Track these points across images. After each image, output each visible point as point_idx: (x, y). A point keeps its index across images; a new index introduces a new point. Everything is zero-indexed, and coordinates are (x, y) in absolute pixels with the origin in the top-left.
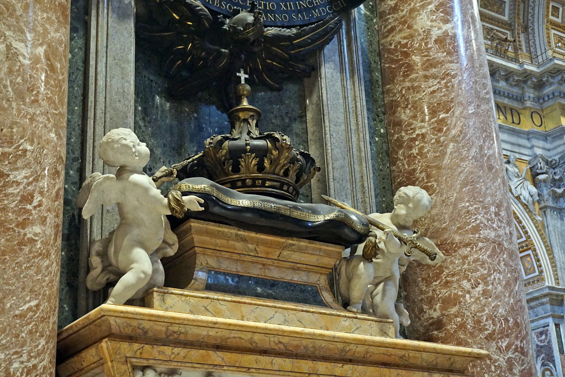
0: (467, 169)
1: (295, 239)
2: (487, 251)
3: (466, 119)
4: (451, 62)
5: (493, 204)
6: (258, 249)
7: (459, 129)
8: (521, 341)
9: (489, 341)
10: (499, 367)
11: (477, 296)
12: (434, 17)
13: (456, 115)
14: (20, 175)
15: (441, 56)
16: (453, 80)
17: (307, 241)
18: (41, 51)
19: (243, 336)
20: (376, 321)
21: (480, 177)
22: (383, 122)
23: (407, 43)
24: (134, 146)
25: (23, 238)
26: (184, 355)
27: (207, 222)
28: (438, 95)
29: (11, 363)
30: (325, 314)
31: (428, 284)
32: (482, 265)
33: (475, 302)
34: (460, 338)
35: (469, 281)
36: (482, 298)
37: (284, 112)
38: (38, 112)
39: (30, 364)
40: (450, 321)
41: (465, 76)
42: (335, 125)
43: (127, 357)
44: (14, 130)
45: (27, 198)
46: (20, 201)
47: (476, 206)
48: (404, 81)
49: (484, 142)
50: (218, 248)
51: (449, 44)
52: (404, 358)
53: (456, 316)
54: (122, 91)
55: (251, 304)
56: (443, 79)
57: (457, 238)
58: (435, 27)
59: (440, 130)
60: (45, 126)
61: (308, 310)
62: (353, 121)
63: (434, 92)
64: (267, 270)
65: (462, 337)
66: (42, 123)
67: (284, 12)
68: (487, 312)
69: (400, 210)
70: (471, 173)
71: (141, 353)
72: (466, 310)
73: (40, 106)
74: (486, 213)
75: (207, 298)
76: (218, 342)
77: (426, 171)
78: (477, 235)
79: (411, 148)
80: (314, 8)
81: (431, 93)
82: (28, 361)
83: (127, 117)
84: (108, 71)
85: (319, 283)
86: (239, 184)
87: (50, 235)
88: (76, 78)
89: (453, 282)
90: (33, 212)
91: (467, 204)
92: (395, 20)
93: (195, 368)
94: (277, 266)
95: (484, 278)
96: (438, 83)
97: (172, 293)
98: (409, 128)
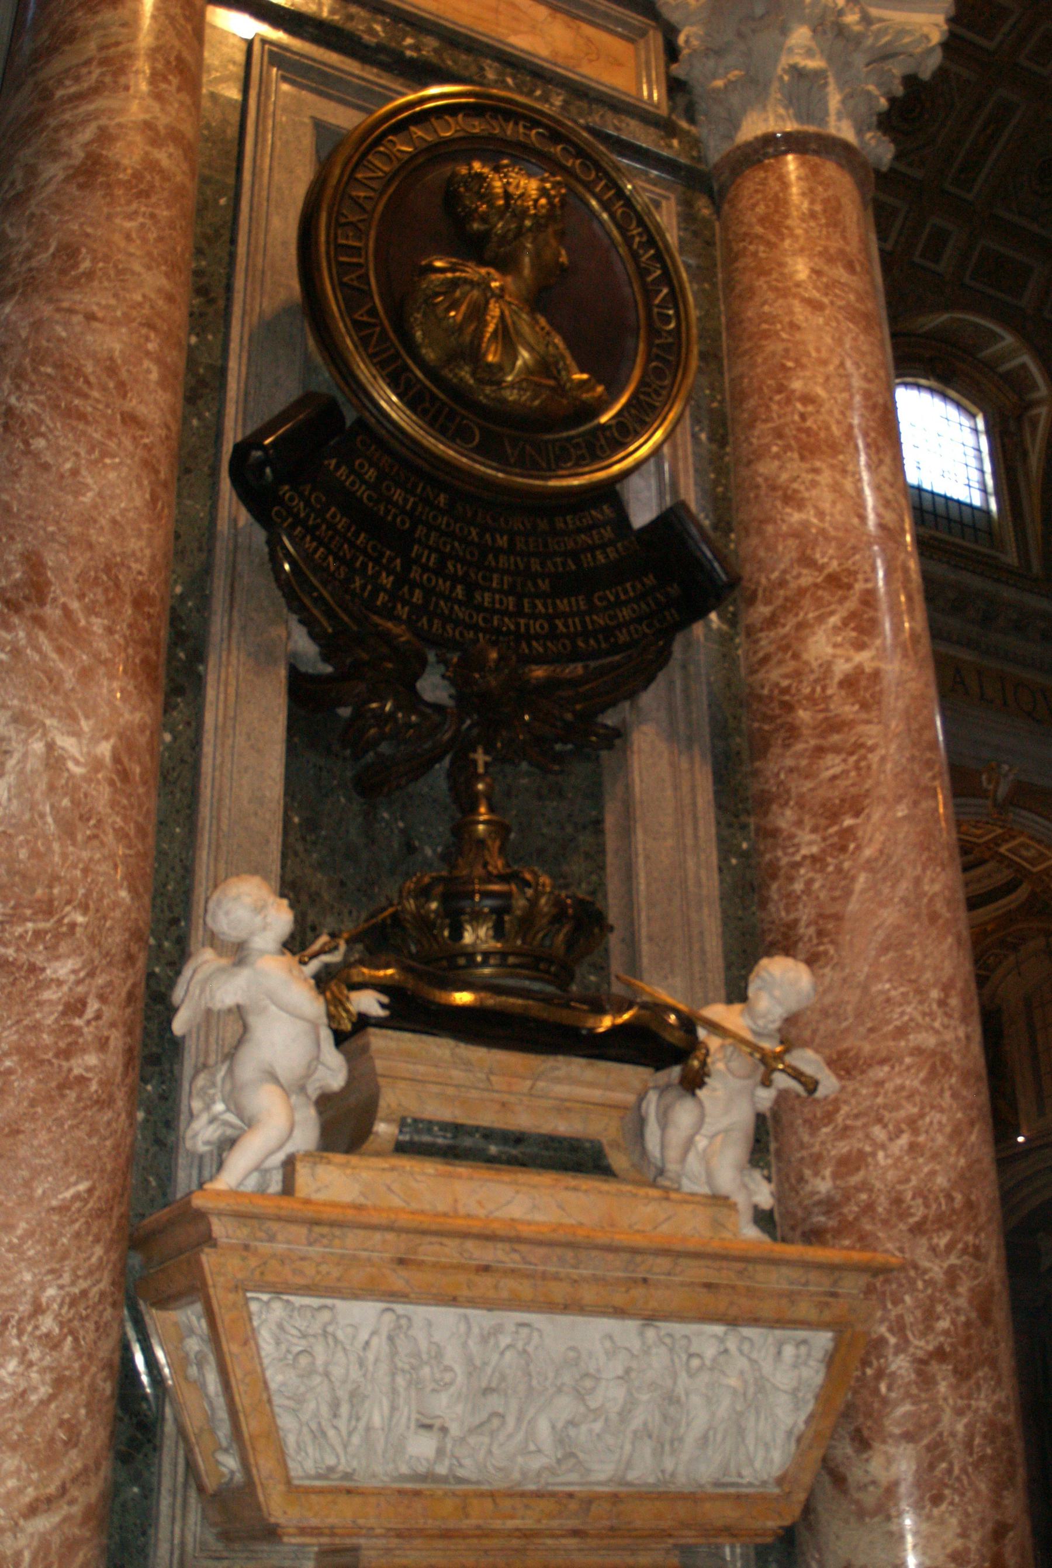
2: (919, 1071)
4: (868, 722)
5: (934, 985)
8: (976, 1235)
11: (897, 1152)
12: (839, 639)
15: (849, 710)
16: (870, 756)
18: (105, 749)
21: (913, 935)
23: (789, 687)
25: (67, 1077)
28: (842, 783)
29: (42, 1287)
31: (814, 1130)
33: (895, 1166)
35: (885, 1126)
38: (98, 856)
39: (76, 1290)
41: (893, 747)
44: (56, 891)
46: (64, 1013)
48: (783, 756)
51: (866, 689)
56: (852, 754)
57: (867, 1048)
58: (841, 656)
59: (843, 849)
62: (689, 831)
63: (834, 778)
65: (868, 1227)
66: (105, 874)
68: (914, 1181)
71: (262, 1273)
74: (921, 1002)
79: (791, 879)
80: (619, 627)
82: (73, 1283)
87: (116, 1068)
90: (86, 1030)
91: (887, 986)
92: (770, 643)
95: (912, 1123)
98: (788, 843)
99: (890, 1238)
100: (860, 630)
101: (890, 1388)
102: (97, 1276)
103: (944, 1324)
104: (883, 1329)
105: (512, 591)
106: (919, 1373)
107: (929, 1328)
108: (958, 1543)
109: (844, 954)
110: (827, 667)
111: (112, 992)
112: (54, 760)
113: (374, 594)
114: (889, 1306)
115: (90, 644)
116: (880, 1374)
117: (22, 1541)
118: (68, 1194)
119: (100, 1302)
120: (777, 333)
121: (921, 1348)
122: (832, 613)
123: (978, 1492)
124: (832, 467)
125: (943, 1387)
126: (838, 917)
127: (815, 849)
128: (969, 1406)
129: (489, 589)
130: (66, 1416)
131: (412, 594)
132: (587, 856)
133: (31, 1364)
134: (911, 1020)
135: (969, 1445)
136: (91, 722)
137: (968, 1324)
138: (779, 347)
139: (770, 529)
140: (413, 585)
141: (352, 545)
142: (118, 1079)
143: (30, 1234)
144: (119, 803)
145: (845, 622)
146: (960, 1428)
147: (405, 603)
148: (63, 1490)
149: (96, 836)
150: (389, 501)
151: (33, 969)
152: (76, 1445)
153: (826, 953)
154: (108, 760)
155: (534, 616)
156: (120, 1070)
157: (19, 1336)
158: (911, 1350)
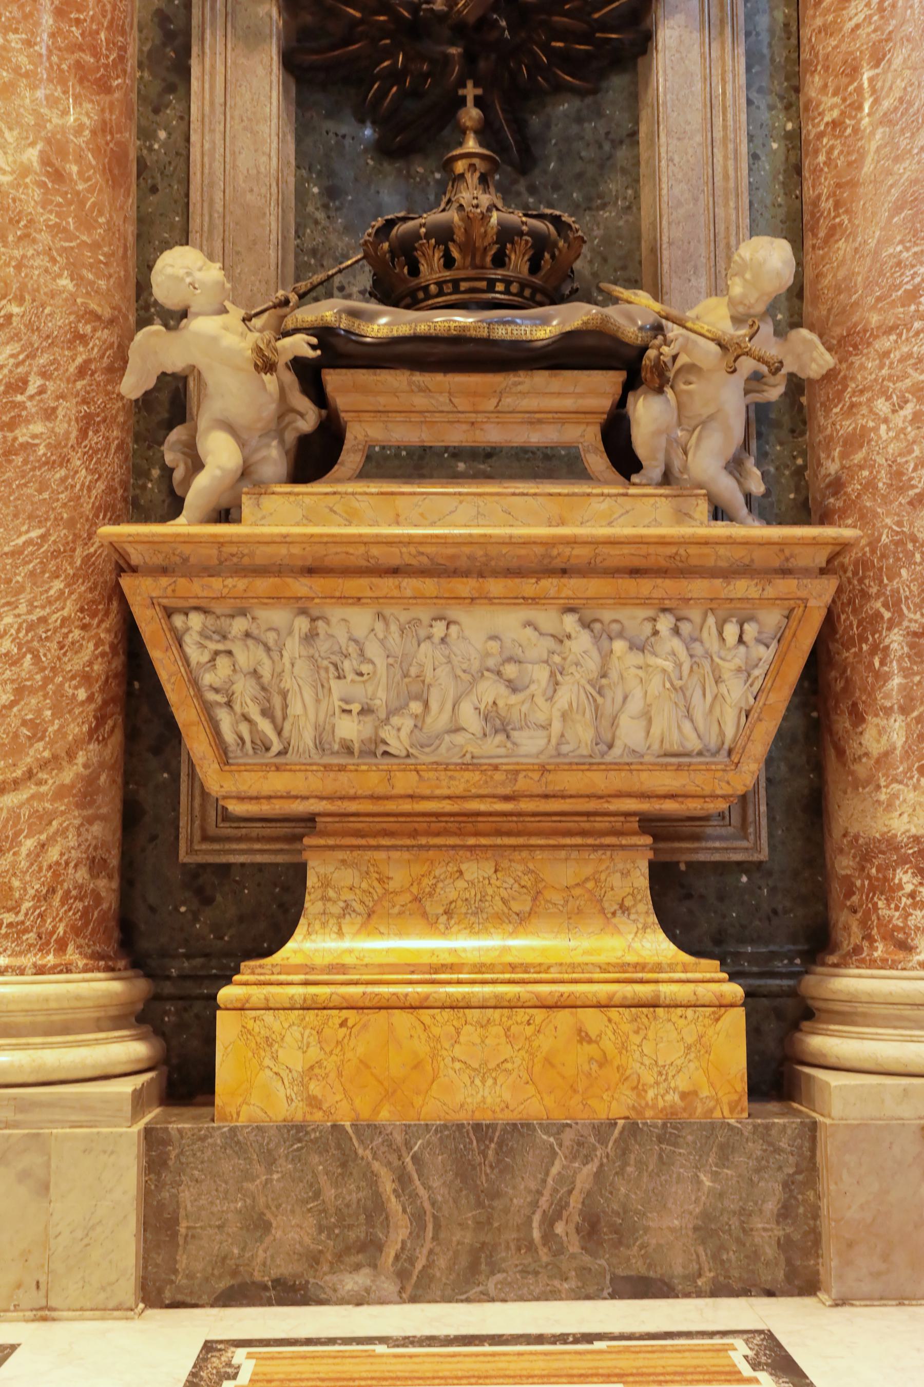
0: (906, 176)
1: (521, 373)
3: (915, 69)
6: (455, 400)
7: (898, 95)
9: (914, 507)
11: (901, 425)
13: (893, 67)
17: (546, 373)
18: (32, 155)
19: (351, 551)
20: (666, 496)
22: (794, 108)
24: (188, 274)
25: (13, 445)
26: (244, 587)
27: (352, 371)
30: (560, 494)
31: (828, 411)
32: (916, 364)
33: (896, 437)
34: (865, 507)
35: (888, 398)
36: (909, 429)
37: (602, 131)
38: (30, 252)
40: (853, 478)
42: (679, 139)
43: (152, 598)
47: (916, 249)
48: (814, 16)
50: (381, 408)
52: (678, 558)
53: (861, 468)
54: (255, 171)
55: (414, 494)
57: (874, 319)
60: (46, 271)
61: (525, 491)
63: (858, 26)
64: (478, 432)
65: (868, 504)
66: (40, 267)
69: (737, 288)
71: (174, 591)
72: (878, 453)
73: (34, 241)
75: (335, 493)
76: (309, 562)
77: (834, 194)
78: (913, 307)
79: (816, 152)
81: (853, 30)
82: (29, 612)
83: (265, 214)
84: (228, 144)
85: (581, 440)
86: (421, 295)
87: (67, 434)
88: (175, 168)
89: (860, 404)
90: (29, 404)
91: (899, 248)
93: (266, 604)
94: (498, 423)
96: (866, 6)
97: (273, 493)
99: (888, 514)
101: (882, 663)
102: (58, 605)
106: (912, 646)
109: (857, 222)
111: (55, 369)
114: (886, 581)
115: (10, 61)
116: (875, 649)
119: (62, 626)
121: (916, 621)
127: (835, 113)
130: (30, 716)
132: (624, 171)
136: (15, 133)
142: (72, 441)
144: (52, 202)
148: (30, 774)
149: (27, 236)
152: (42, 739)
153: (841, 224)
154: (36, 166)
156: (74, 434)
158: (905, 623)
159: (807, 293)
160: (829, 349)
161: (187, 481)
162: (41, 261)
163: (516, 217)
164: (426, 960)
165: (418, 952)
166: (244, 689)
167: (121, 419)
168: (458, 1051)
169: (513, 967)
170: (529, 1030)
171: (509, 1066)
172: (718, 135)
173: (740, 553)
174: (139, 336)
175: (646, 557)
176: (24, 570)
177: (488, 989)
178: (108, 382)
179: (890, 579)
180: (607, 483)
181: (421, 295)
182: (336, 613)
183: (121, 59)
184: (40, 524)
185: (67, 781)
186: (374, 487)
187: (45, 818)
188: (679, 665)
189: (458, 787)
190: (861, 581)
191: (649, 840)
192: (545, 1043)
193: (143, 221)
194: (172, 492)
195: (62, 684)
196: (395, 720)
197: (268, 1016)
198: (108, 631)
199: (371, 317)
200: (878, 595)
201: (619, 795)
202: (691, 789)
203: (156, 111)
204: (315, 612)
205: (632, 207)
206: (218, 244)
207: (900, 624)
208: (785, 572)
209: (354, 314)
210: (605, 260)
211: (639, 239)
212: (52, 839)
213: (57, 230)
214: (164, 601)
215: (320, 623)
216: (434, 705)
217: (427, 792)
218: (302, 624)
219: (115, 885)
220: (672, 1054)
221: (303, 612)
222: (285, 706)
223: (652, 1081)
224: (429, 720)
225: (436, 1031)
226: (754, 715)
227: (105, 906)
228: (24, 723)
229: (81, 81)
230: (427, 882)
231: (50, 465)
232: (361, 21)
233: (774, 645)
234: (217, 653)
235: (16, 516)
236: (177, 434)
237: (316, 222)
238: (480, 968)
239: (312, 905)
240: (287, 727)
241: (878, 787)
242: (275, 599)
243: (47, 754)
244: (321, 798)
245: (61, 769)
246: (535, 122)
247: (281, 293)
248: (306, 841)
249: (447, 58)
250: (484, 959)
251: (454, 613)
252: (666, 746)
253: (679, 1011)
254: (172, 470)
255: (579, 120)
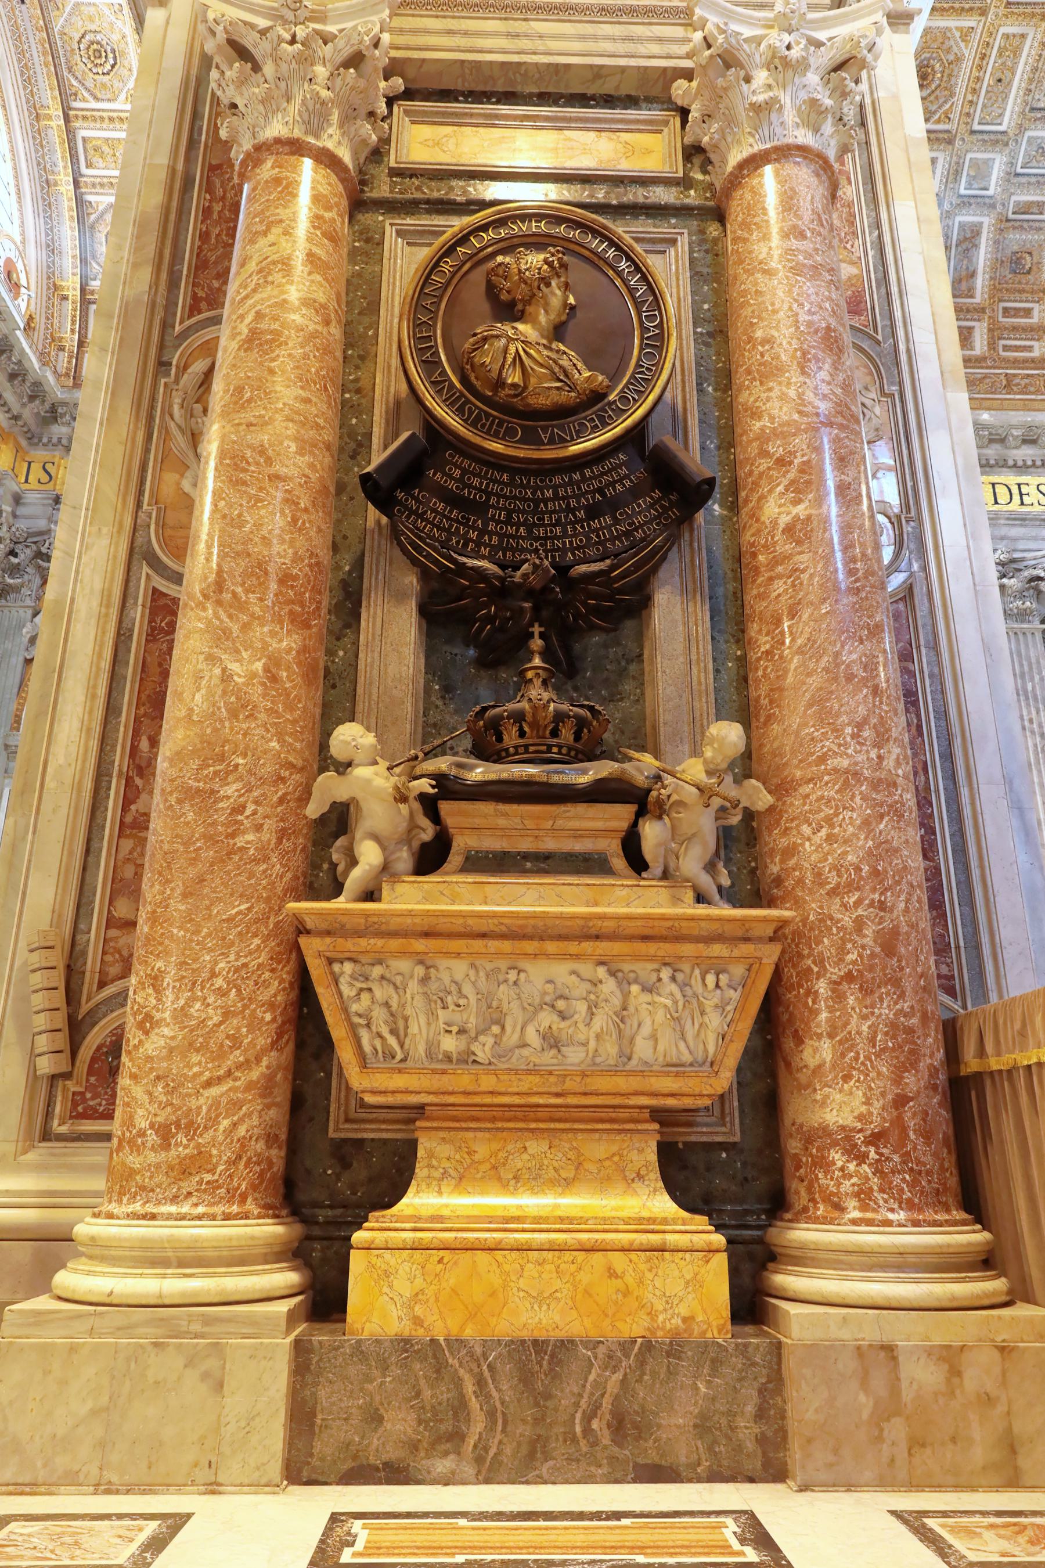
5: (849, 724)
8: (881, 894)
10: (843, 928)
14: (231, 790)
18: (259, 666)
21: (832, 692)
29: (216, 963)
31: (770, 832)
33: (816, 850)
35: (810, 825)
45: (240, 809)
49: (842, 646)
53: (794, 870)
57: (798, 774)
63: (779, 595)
67: (596, 543)
68: (830, 860)
69: (709, 753)
70: (821, 689)
73: (256, 719)
74: (837, 737)
79: (757, 669)
80: (636, 529)
82: (237, 960)
87: (269, 840)
95: (829, 821)
99: (813, 901)
100: (797, 491)
101: (814, 1002)
103: (852, 957)
104: (809, 962)
105: (558, 522)
106: (833, 991)
107: (841, 960)
108: (863, 1109)
110: (775, 522)
112: (226, 677)
113: (466, 545)
116: (808, 992)
117: (202, 1100)
118: (234, 912)
120: (748, 302)
122: (778, 485)
123: (879, 1073)
124: (780, 383)
125: (851, 1000)
126: (781, 689)
127: (768, 646)
128: (873, 1013)
129: (545, 526)
131: (490, 540)
132: (634, 678)
133: (208, 1005)
134: (829, 750)
135: (872, 1041)
137: (873, 955)
138: (750, 309)
139: (744, 438)
140: (491, 534)
141: (448, 518)
142: (272, 845)
143: (209, 935)
145: (787, 490)
146: (865, 1028)
147: (486, 546)
148: (229, 1073)
150: (470, 486)
151: (213, 792)
155: (575, 535)
156: (274, 841)
157: (202, 990)
159: (754, 756)
160: (770, 792)
161: (346, 873)
162: (260, 731)
163: (565, 707)
164: (500, 1213)
165: (494, 1207)
166: (379, 1015)
167: (305, 831)
168: (522, 1283)
169: (562, 1220)
170: (573, 1268)
171: (558, 1295)
172: (694, 657)
173: (715, 926)
174: (320, 779)
175: (652, 927)
176: (234, 931)
177: (544, 1236)
178: (298, 807)
179: (817, 945)
180: (626, 877)
181: (504, 754)
182: (443, 963)
183: (318, 608)
184: (248, 901)
185: (255, 1078)
186: (470, 878)
187: (237, 1105)
188: (676, 1002)
189: (524, 1087)
190: (797, 946)
191: (656, 1126)
192: (584, 1277)
193: (326, 706)
194: (335, 878)
195: (255, 1010)
196: (482, 1038)
197: (387, 1254)
198: (288, 973)
199: (471, 768)
200: (809, 956)
201: (637, 1093)
202: (685, 1090)
203: (338, 639)
204: (429, 963)
205: (640, 700)
206: (373, 720)
207: (824, 975)
208: (747, 939)
209: (460, 766)
210: (623, 732)
211: (645, 720)
212: (241, 1120)
213: (270, 711)
214: (328, 954)
215: (432, 970)
216: (508, 1029)
217: (503, 1090)
218: (420, 971)
219: (283, 1153)
220: (675, 1287)
221: (421, 962)
222: (407, 1027)
223: (661, 1308)
224: (505, 1039)
225: (506, 1267)
226: (728, 1038)
227: (275, 1169)
228: (228, 1037)
229: (292, 621)
230: (502, 1155)
231: (257, 861)
232: (468, 587)
233: (740, 989)
234: (361, 990)
235: (232, 895)
236: (341, 842)
237: (437, 707)
238: (538, 1220)
239: (421, 1171)
240: (407, 1042)
241: (815, 1090)
242: (403, 954)
243: (241, 1059)
244: (429, 1093)
245: (250, 1069)
246: (577, 647)
247: (413, 752)
248: (418, 1124)
249: (522, 609)
250: (543, 1213)
251: (523, 964)
252: (668, 1059)
253: (681, 1254)
254: (336, 865)
255: (606, 646)
